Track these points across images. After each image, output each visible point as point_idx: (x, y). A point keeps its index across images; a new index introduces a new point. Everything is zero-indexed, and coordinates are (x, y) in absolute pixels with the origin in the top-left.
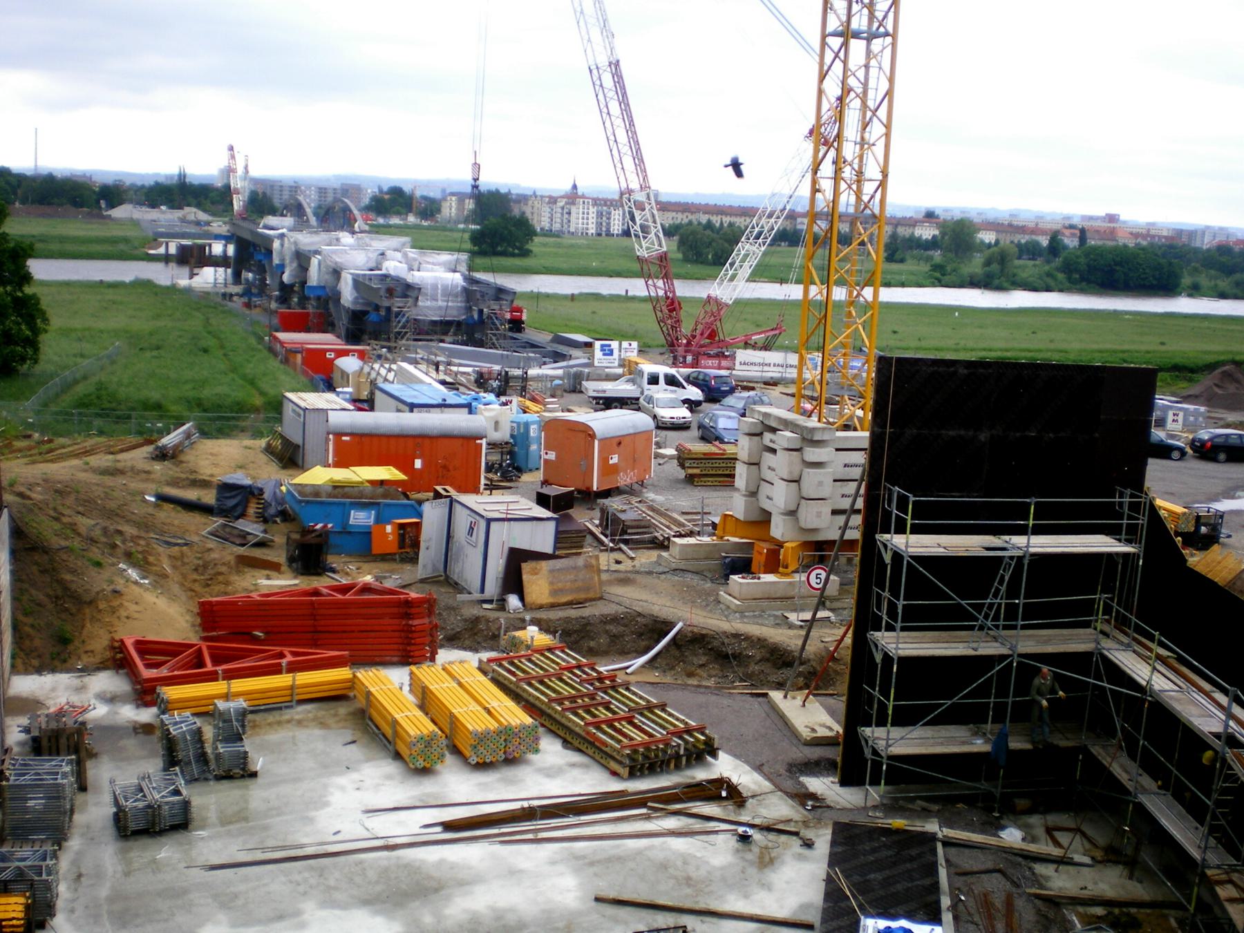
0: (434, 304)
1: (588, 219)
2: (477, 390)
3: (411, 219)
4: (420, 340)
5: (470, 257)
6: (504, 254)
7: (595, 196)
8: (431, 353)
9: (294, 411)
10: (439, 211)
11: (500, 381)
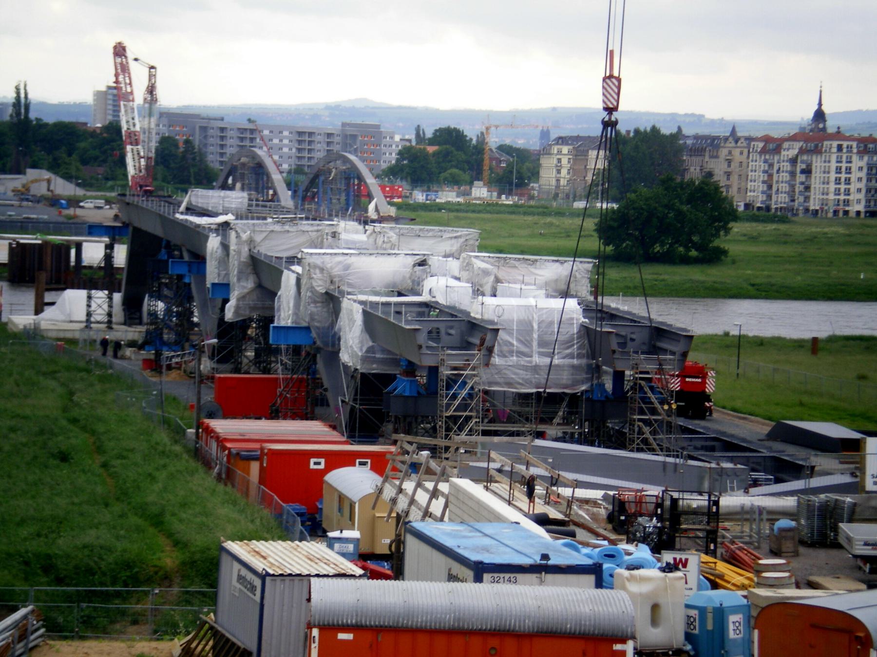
0: (524, 361)
1: (848, 181)
2: (613, 537)
3: (480, 192)
4: (496, 433)
5: (597, 267)
7: (865, 134)
8: (519, 460)
9: (241, 578)
10: (535, 174)
11: (660, 518)
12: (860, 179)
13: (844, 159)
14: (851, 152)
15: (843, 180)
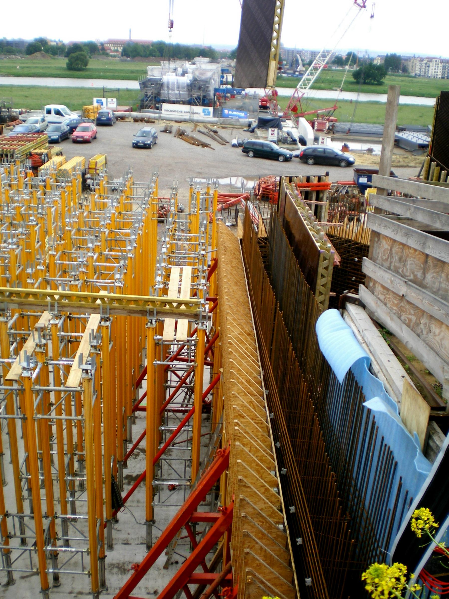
6: (368, 84)
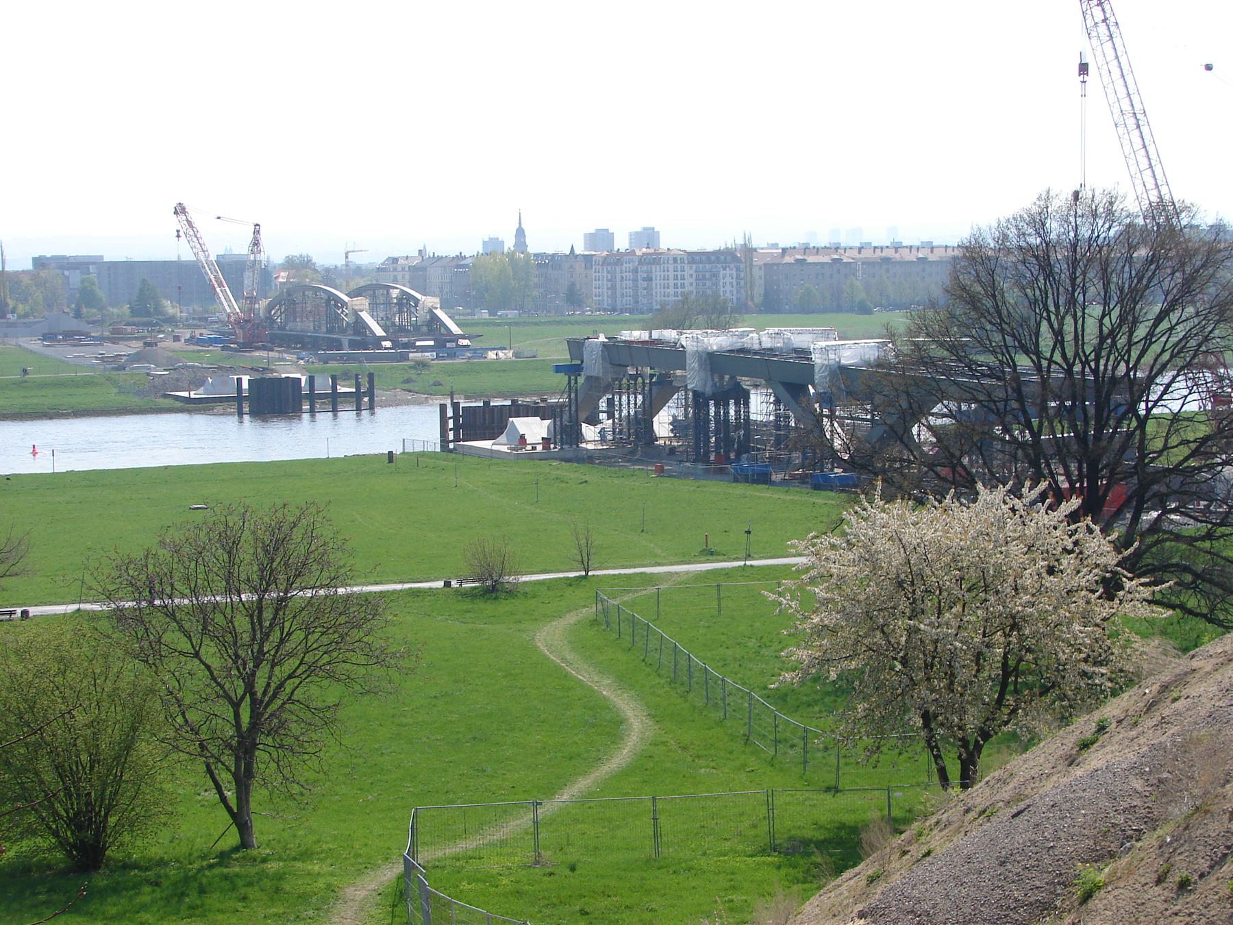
12: (691, 284)
13: (679, 269)
14: (684, 263)
15: (679, 285)
